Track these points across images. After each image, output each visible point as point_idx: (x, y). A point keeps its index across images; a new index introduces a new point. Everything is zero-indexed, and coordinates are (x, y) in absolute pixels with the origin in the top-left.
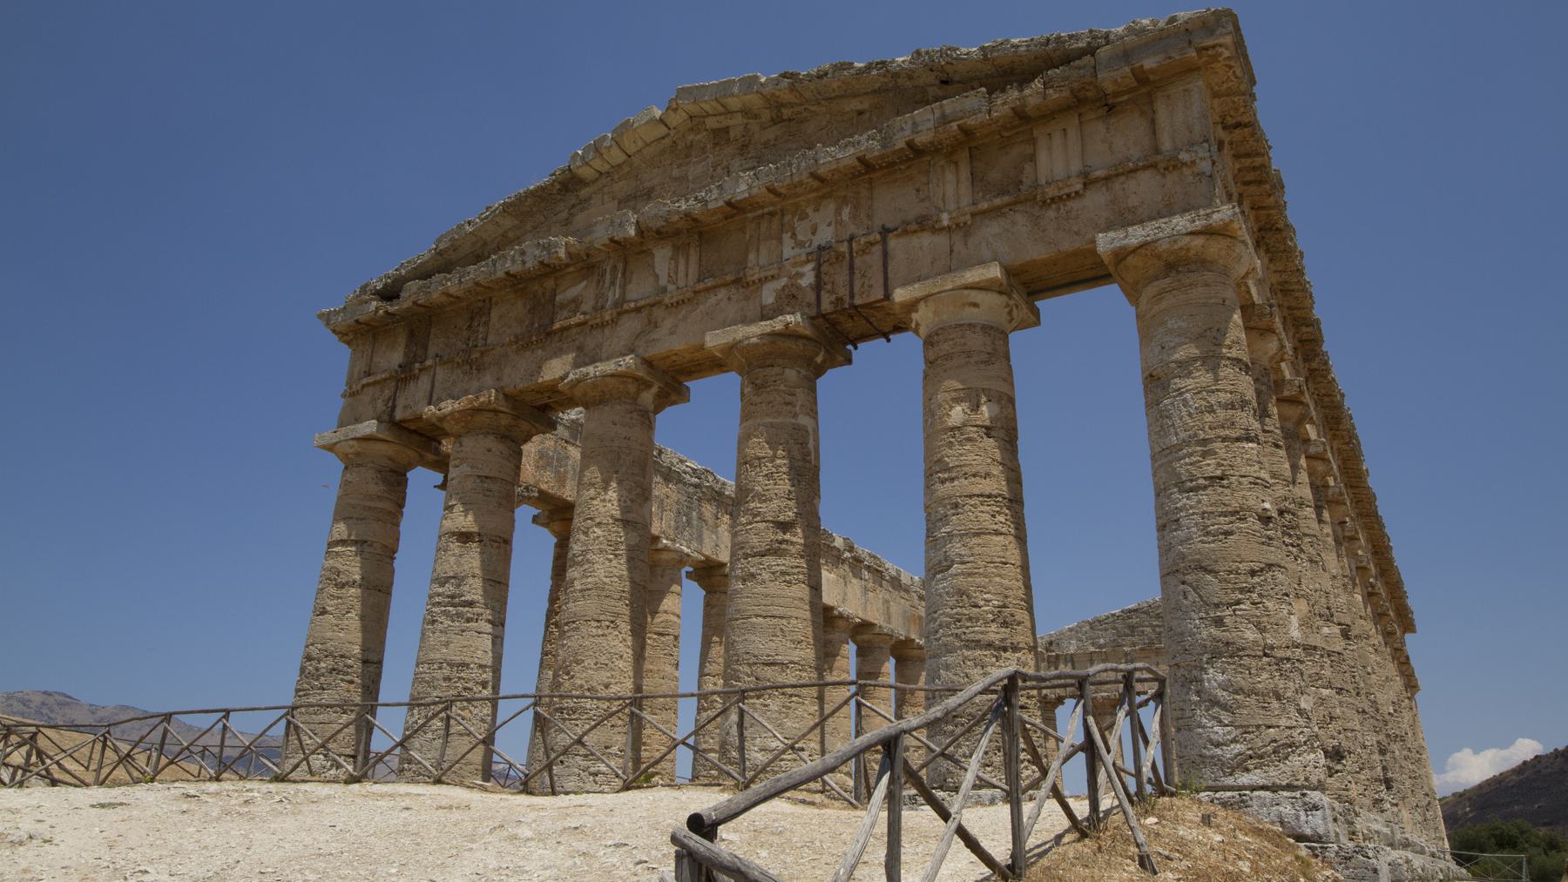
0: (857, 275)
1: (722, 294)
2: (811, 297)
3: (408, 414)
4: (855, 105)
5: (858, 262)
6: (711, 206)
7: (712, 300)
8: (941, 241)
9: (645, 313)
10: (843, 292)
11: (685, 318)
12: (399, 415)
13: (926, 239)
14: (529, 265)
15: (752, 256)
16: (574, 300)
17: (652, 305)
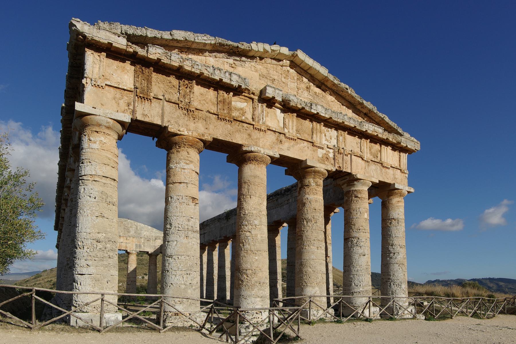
0: (344, 162)
1: (306, 143)
2: (333, 162)
3: (147, 120)
4: (343, 101)
5: (345, 157)
6: (313, 111)
7: (302, 145)
8: (363, 162)
9: (277, 134)
10: (341, 165)
11: (293, 146)
12: (140, 117)
13: (360, 159)
14: (232, 83)
15: (315, 136)
16: (242, 109)
17: (280, 133)
